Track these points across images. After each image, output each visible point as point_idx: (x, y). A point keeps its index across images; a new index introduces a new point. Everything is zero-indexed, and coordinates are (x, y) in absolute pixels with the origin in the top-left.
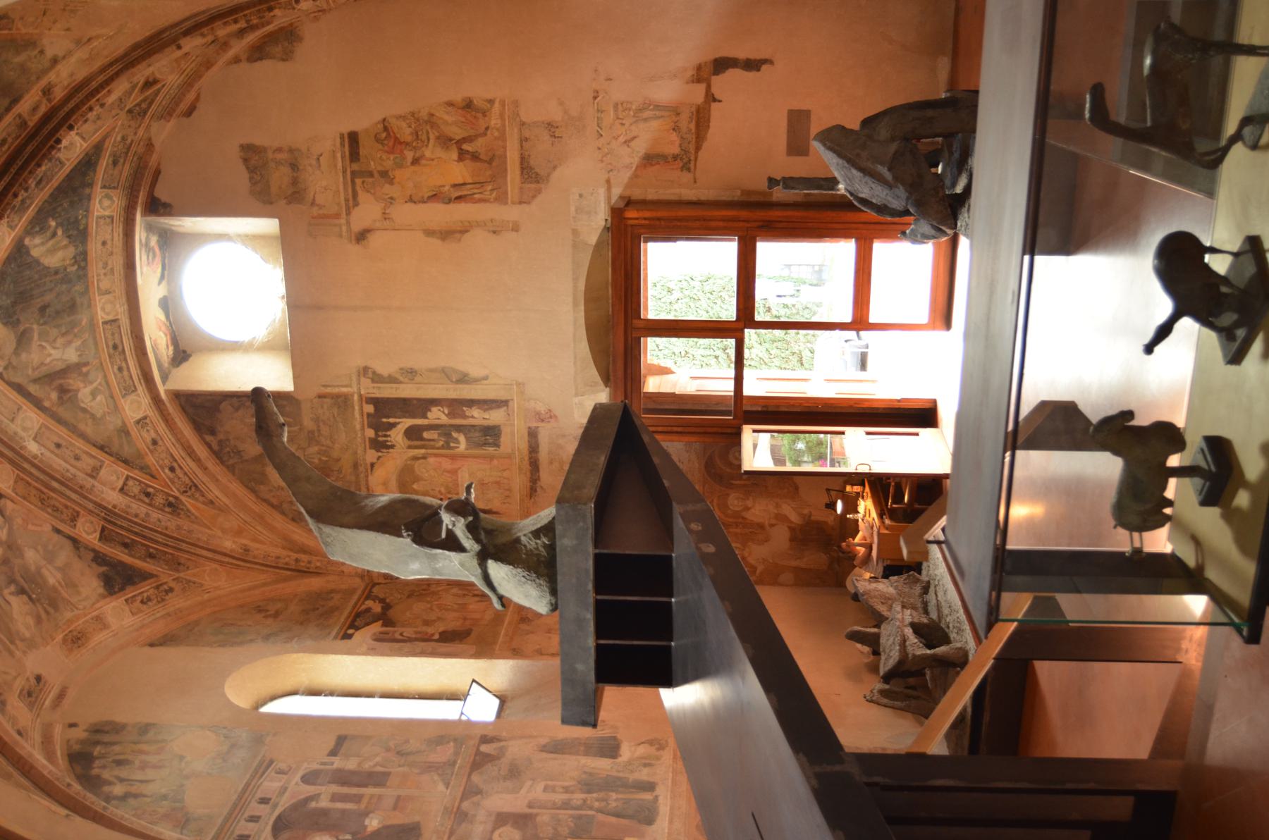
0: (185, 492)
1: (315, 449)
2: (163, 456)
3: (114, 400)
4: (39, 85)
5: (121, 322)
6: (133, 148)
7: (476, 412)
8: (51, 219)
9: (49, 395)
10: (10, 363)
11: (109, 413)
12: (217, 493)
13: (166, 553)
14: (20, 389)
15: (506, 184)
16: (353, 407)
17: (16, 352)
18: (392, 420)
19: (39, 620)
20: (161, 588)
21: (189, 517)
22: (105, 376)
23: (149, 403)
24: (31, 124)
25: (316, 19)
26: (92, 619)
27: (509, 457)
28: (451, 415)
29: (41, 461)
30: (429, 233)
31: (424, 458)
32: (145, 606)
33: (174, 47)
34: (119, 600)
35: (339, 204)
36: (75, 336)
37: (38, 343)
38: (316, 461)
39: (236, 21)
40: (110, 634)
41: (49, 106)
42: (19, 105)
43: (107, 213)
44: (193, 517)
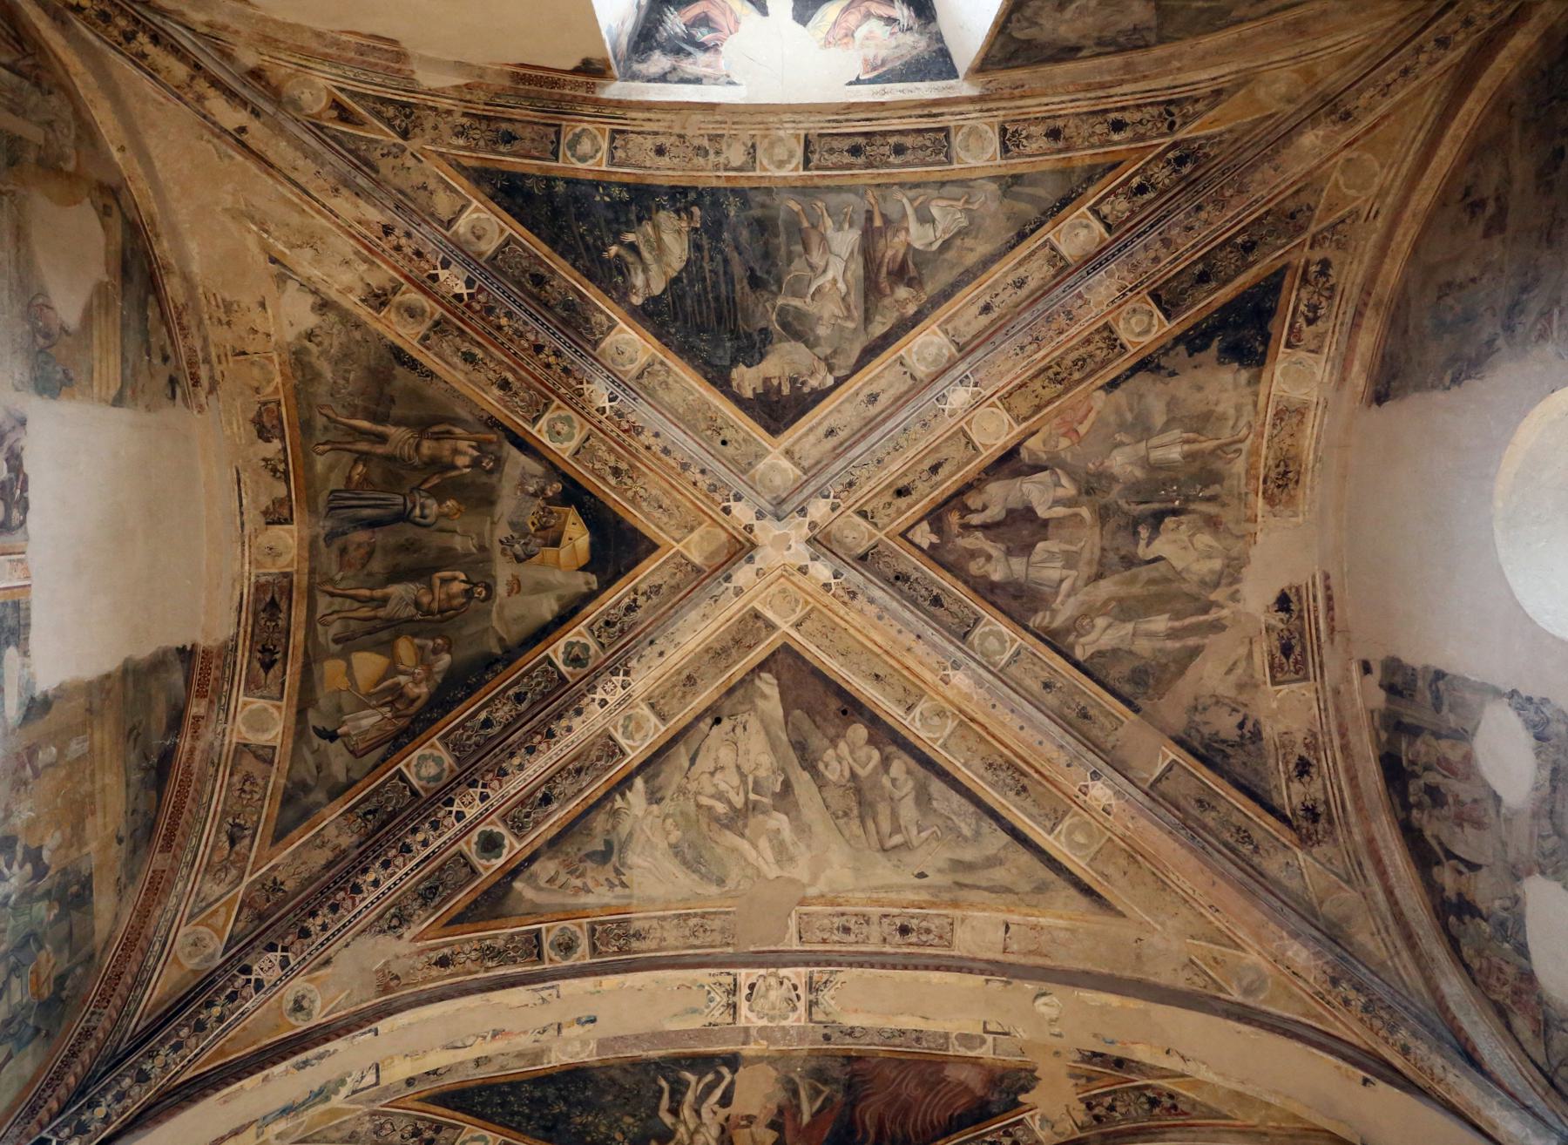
0: (1172, 125)
2: (1085, 129)
3: (952, 182)
4: (369, 320)
6: (479, 109)
8: (605, 255)
11: (967, 202)
13: (1259, 219)
14: (871, 352)
17: (810, 345)
19: (1213, 523)
20: (1312, 277)
21: (1220, 142)
22: (902, 185)
26: (1274, 426)
34: (1280, 356)
36: (814, 226)
37: (808, 300)
41: (406, 285)
42: (406, 347)
43: (605, 145)
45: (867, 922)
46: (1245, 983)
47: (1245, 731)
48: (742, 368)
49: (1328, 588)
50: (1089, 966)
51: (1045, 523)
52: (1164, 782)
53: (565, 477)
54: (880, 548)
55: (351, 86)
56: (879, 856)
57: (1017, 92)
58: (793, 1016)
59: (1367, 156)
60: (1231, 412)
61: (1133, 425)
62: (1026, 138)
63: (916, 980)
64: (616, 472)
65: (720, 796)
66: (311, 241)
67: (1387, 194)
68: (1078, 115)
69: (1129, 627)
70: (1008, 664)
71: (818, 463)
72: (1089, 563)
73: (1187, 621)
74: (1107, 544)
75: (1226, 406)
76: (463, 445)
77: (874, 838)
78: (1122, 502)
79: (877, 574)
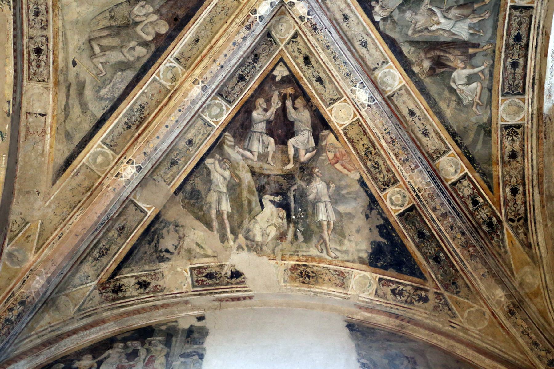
0: (512, 220)
2: (514, 173)
3: (491, 96)
5: (535, 11)
9: (422, 61)
10: (391, 16)
11: (478, 104)
12: (541, 239)
13: (453, 266)
17: (400, 7)
19: (282, 237)
20: (419, 292)
21: (499, 246)
22: (493, 66)
23: (532, 114)
26: (336, 271)
32: (392, 296)
34: (375, 275)
36: (474, 11)
37: (428, 7)
40: (342, 295)
44: (503, 250)
45: (42, 28)
46: (16, 253)
47: (164, 253)
49: (244, 298)
50: (20, 164)
51: (285, 143)
52: (134, 208)
54: (274, 46)
56: (87, 36)
57: (542, 135)
59: (486, 323)
60: (344, 248)
61: (339, 194)
62: (513, 140)
63: (7, 57)
67: (464, 333)
68: (523, 169)
69: (224, 190)
70: (203, 120)
71: (328, 9)
72: (261, 168)
73: (226, 222)
74: (272, 178)
75: (347, 245)
77: (97, 35)
78: (295, 187)
79: (259, 44)
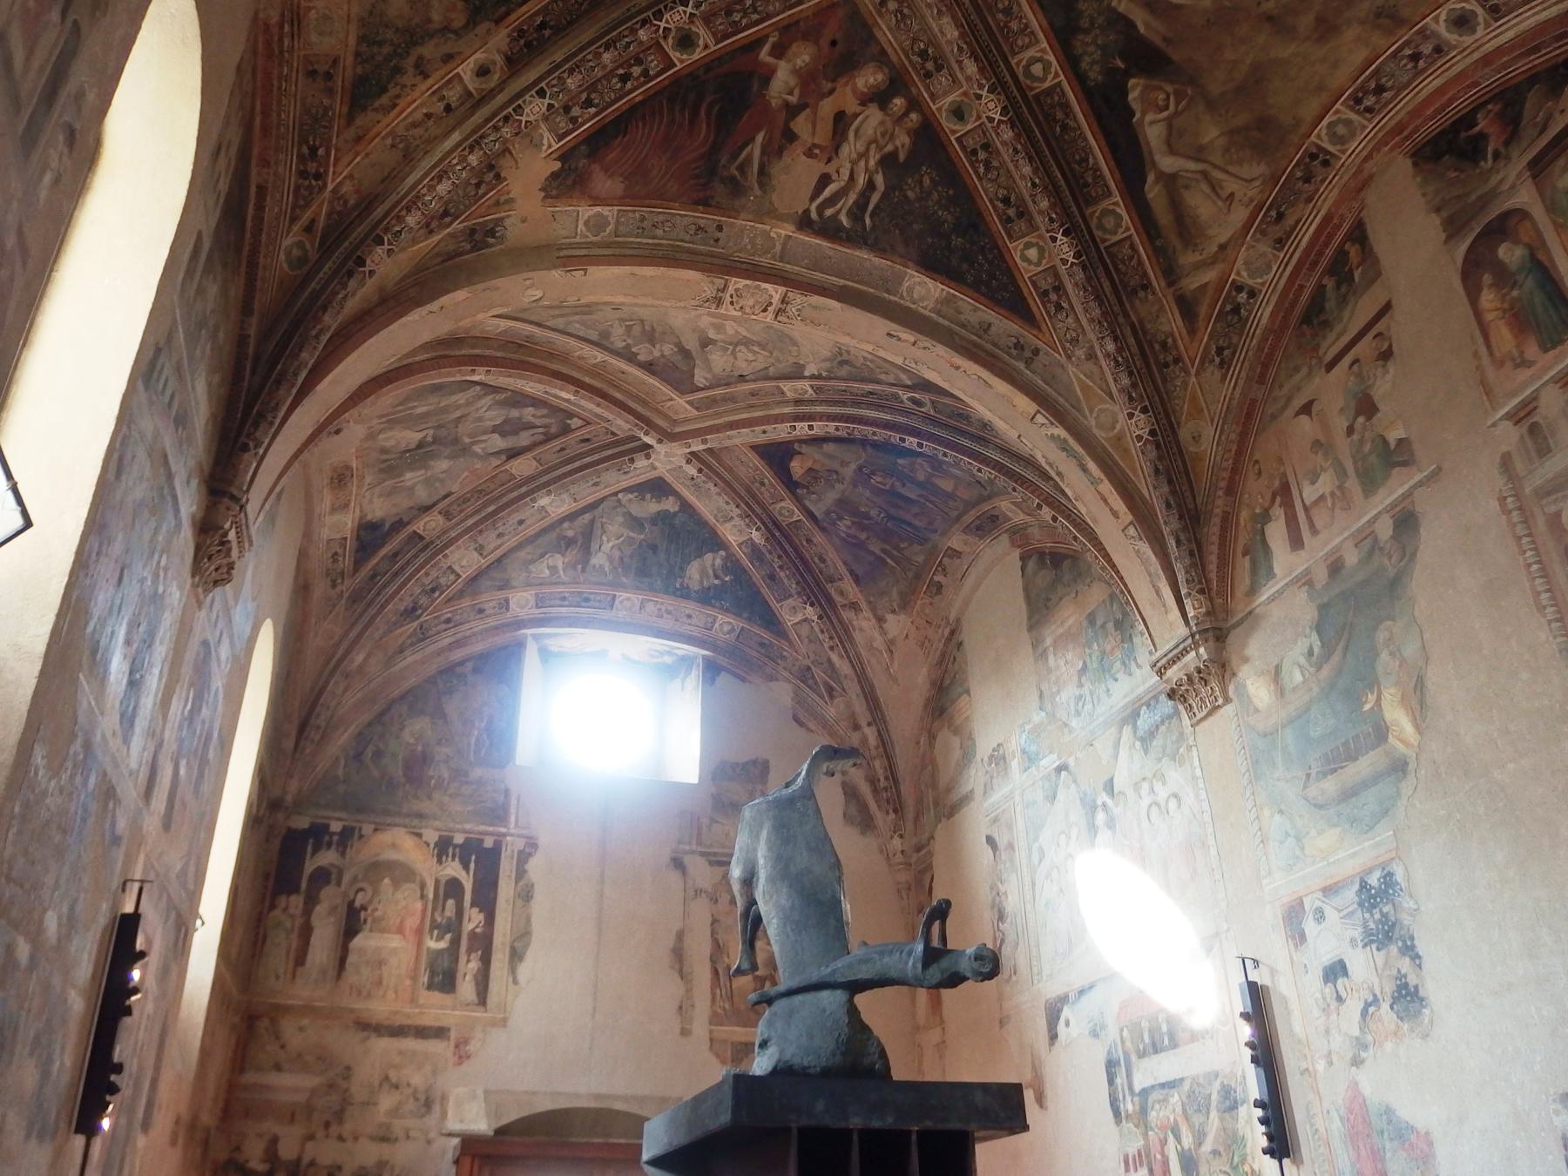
0: (421, 628)
1: (446, 775)
7: (474, 965)
12: (410, 659)
15: (730, 1025)
16: (492, 825)
18: (472, 866)
19: (384, 451)
24: (828, 586)
25: (881, 851)
27: (413, 1001)
28: (473, 935)
29: (526, 504)
30: (680, 936)
31: (423, 897)
33: (870, 720)
35: (711, 846)
36: (615, 568)
38: (431, 773)
39: (886, 778)
43: (717, 625)
48: (672, 510)
53: (794, 494)
55: (821, 702)
58: (740, 286)
60: (375, 500)
64: (763, 484)
65: (755, 353)
66: (871, 648)
76: (843, 528)
